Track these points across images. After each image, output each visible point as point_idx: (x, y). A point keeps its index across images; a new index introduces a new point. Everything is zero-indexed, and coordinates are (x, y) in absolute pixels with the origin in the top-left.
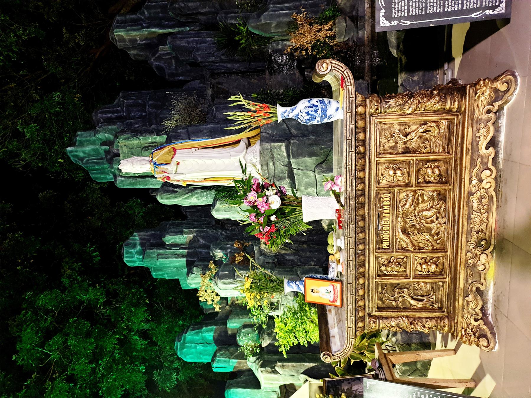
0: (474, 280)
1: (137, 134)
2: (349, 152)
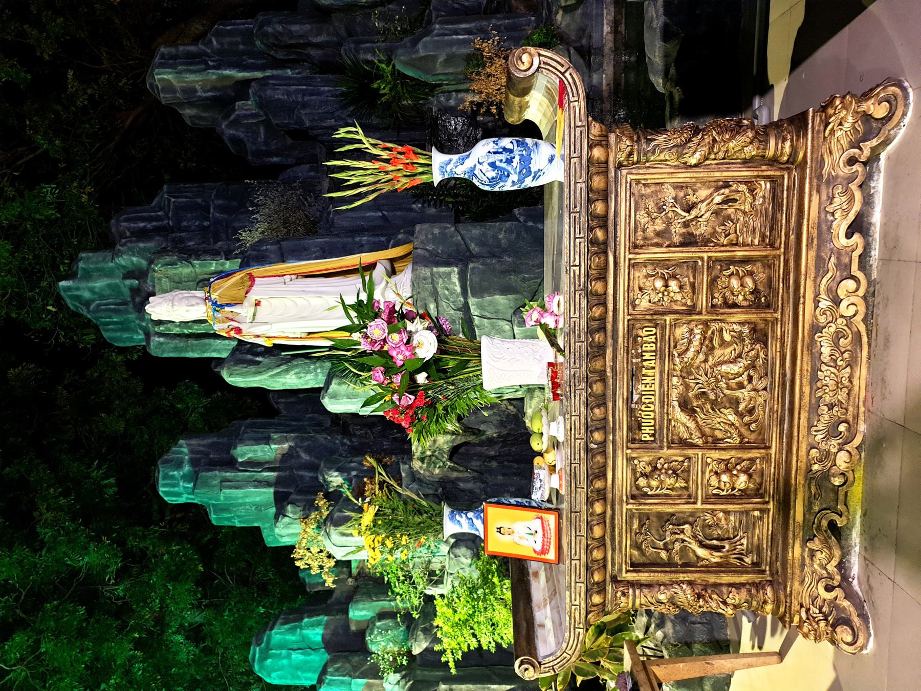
0: (824, 506)
1: (190, 256)
2: (575, 238)
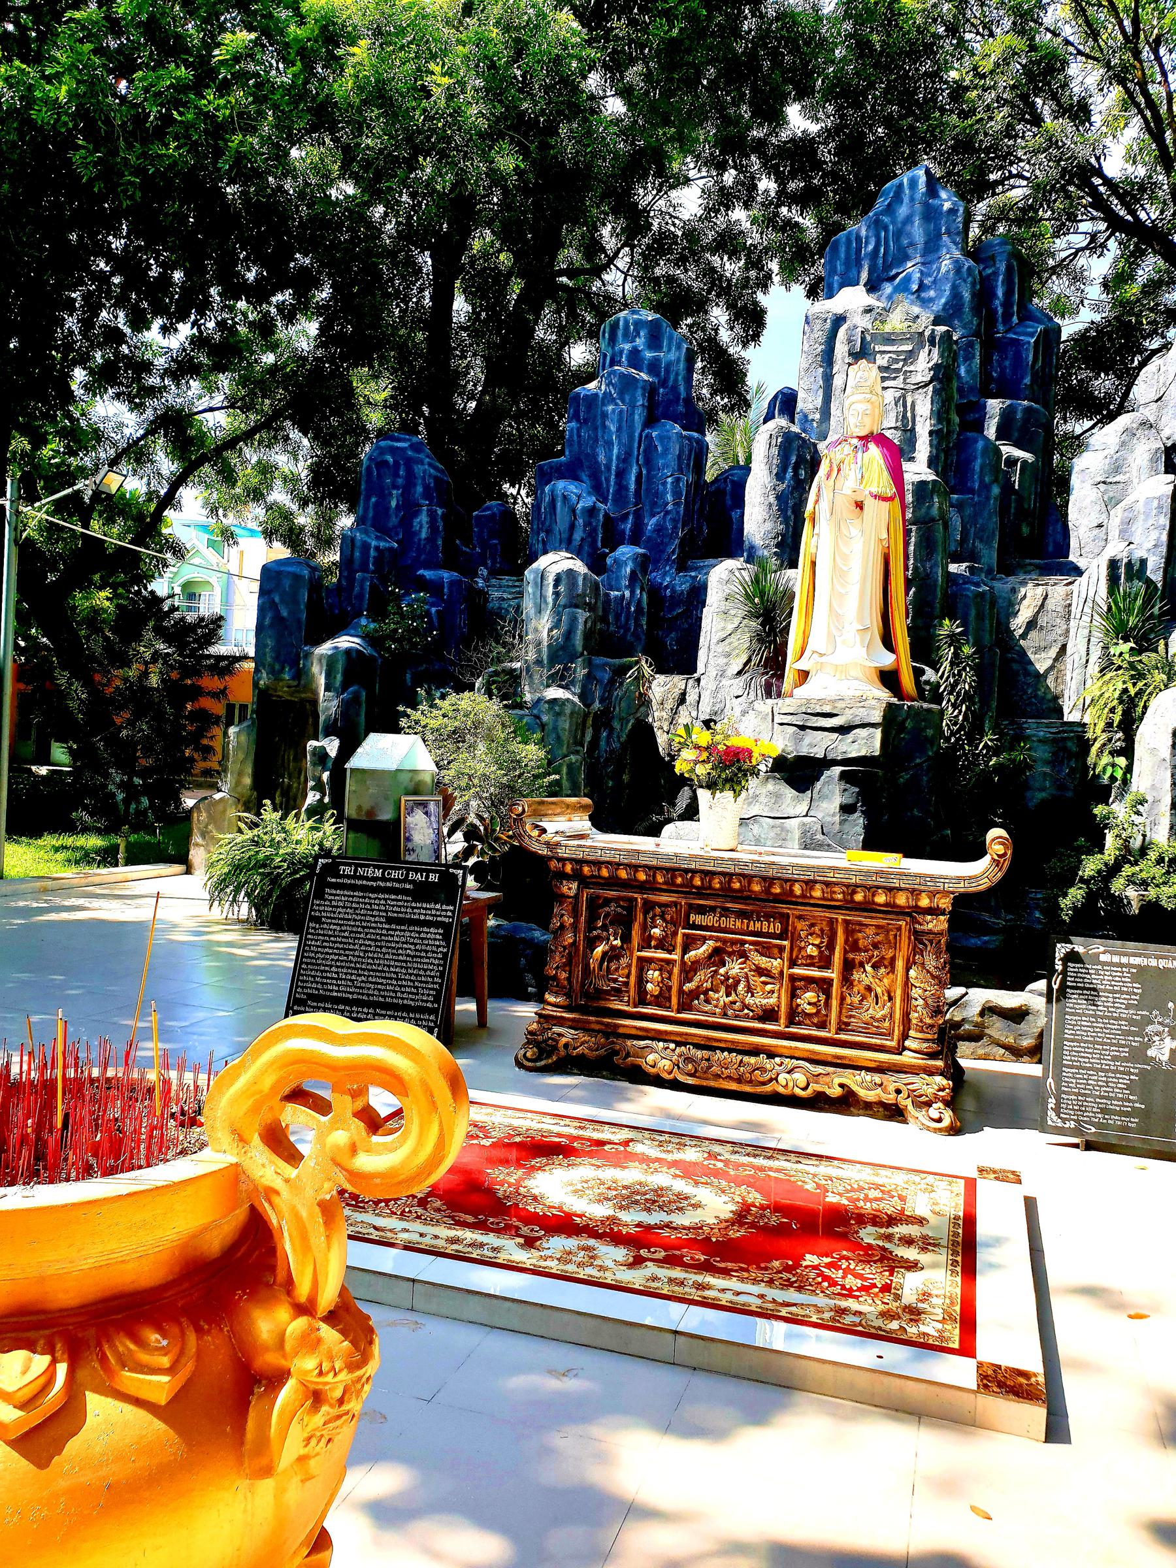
1: (940, 381)
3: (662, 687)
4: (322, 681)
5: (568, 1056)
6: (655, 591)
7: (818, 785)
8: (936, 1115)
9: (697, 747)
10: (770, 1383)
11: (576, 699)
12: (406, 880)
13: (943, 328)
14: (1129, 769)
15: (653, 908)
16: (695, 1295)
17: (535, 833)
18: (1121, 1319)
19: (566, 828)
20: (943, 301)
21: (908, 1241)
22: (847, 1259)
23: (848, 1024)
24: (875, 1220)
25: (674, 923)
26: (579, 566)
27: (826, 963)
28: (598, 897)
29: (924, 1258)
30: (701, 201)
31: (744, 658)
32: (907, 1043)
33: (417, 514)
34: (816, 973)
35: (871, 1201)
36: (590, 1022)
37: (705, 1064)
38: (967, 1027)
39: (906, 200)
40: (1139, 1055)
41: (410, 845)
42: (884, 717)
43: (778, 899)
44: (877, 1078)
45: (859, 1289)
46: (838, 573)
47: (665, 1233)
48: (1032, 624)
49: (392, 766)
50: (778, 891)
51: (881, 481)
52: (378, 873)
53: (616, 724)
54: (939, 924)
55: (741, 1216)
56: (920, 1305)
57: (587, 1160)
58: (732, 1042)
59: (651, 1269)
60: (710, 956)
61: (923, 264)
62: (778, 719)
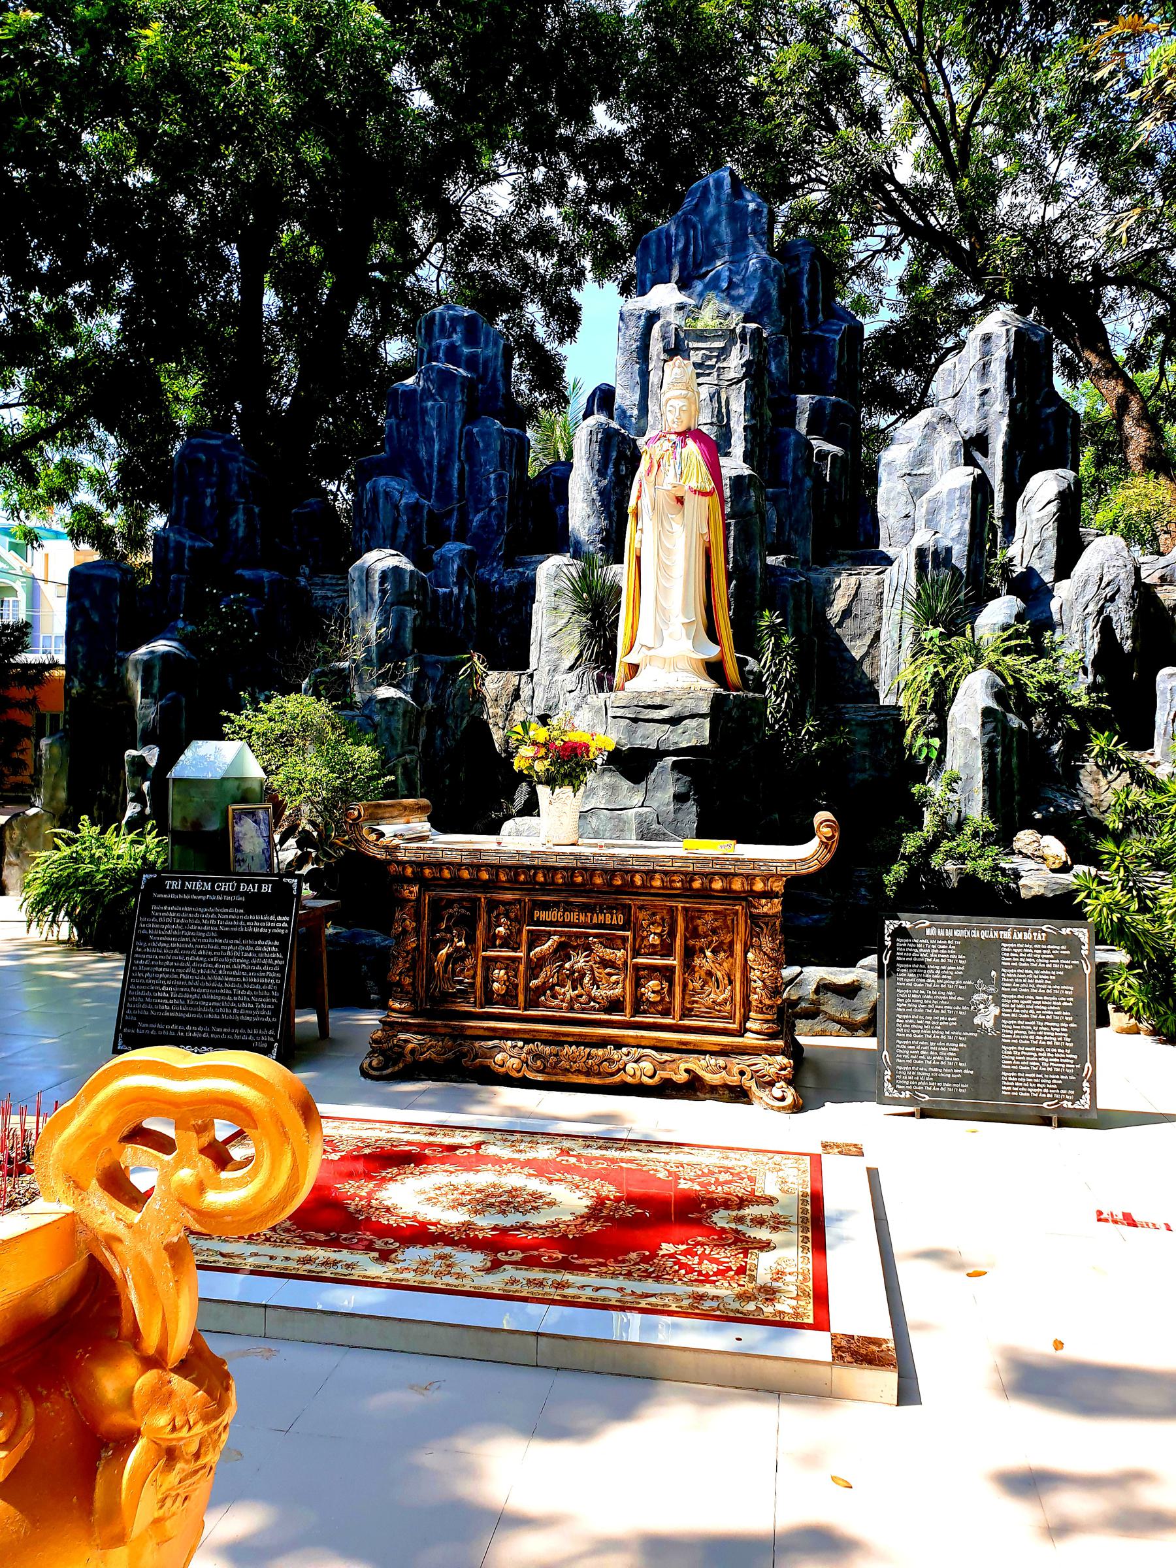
3: (495, 683)
4: (139, 688)
5: (416, 1062)
6: (483, 586)
7: (652, 776)
8: (777, 1092)
9: (534, 743)
10: (633, 1378)
11: (408, 698)
12: (237, 893)
13: (754, 326)
14: (942, 750)
15: (497, 908)
16: (555, 1294)
17: (373, 837)
18: (961, 1276)
19: (406, 832)
20: (752, 298)
21: (760, 1222)
22: (702, 1244)
23: (691, 1010)
24: (726, 1204)
25: (517, 920)
26: (406, 564)
27: (667, 951)
28: (441, 899)
29: (776, 1237)
30: (512, 197)
31: (576, 653)
32: (748, 1025)
33: (235, 511)
34: (659, 962)
35: (721, 1184)
36: (436, 1026)
37: (553, 1059)
38: (803, 1005)
39: (713, 200)
40: (966, 1023)
41: (240, 856)
42: (712, 707)
43: (620, 890)
44: (721, 1061)
45: (715, 1274)
46: (663, 568)
47: (522, 1234)
48: (846, 613)
49: (219, 775)
50: (620, 882)
51: (698, 477)
52: (208, 886)
53: (450, 722)
54: (773, 907)
55: (596, 1210)
56: (775, 1284)
57: (439, 1167)
58: (580, 1035)
59: (510, 1272)
60: (555, 951)
61: (731, 262)
62: (610, 714)
